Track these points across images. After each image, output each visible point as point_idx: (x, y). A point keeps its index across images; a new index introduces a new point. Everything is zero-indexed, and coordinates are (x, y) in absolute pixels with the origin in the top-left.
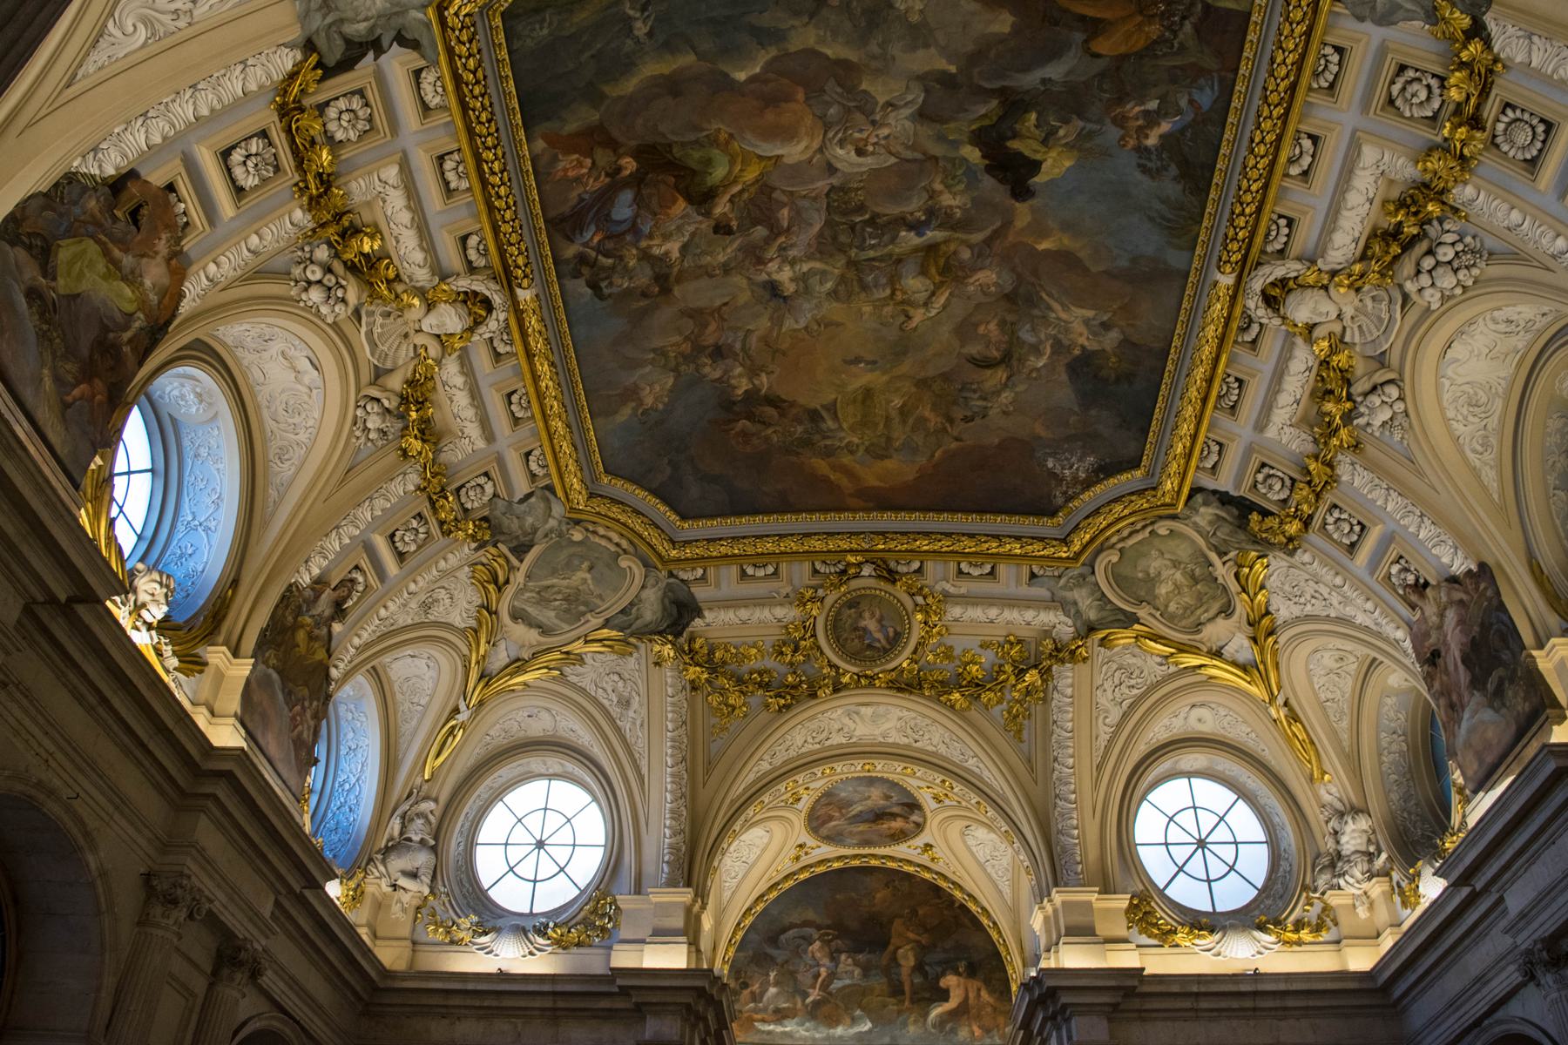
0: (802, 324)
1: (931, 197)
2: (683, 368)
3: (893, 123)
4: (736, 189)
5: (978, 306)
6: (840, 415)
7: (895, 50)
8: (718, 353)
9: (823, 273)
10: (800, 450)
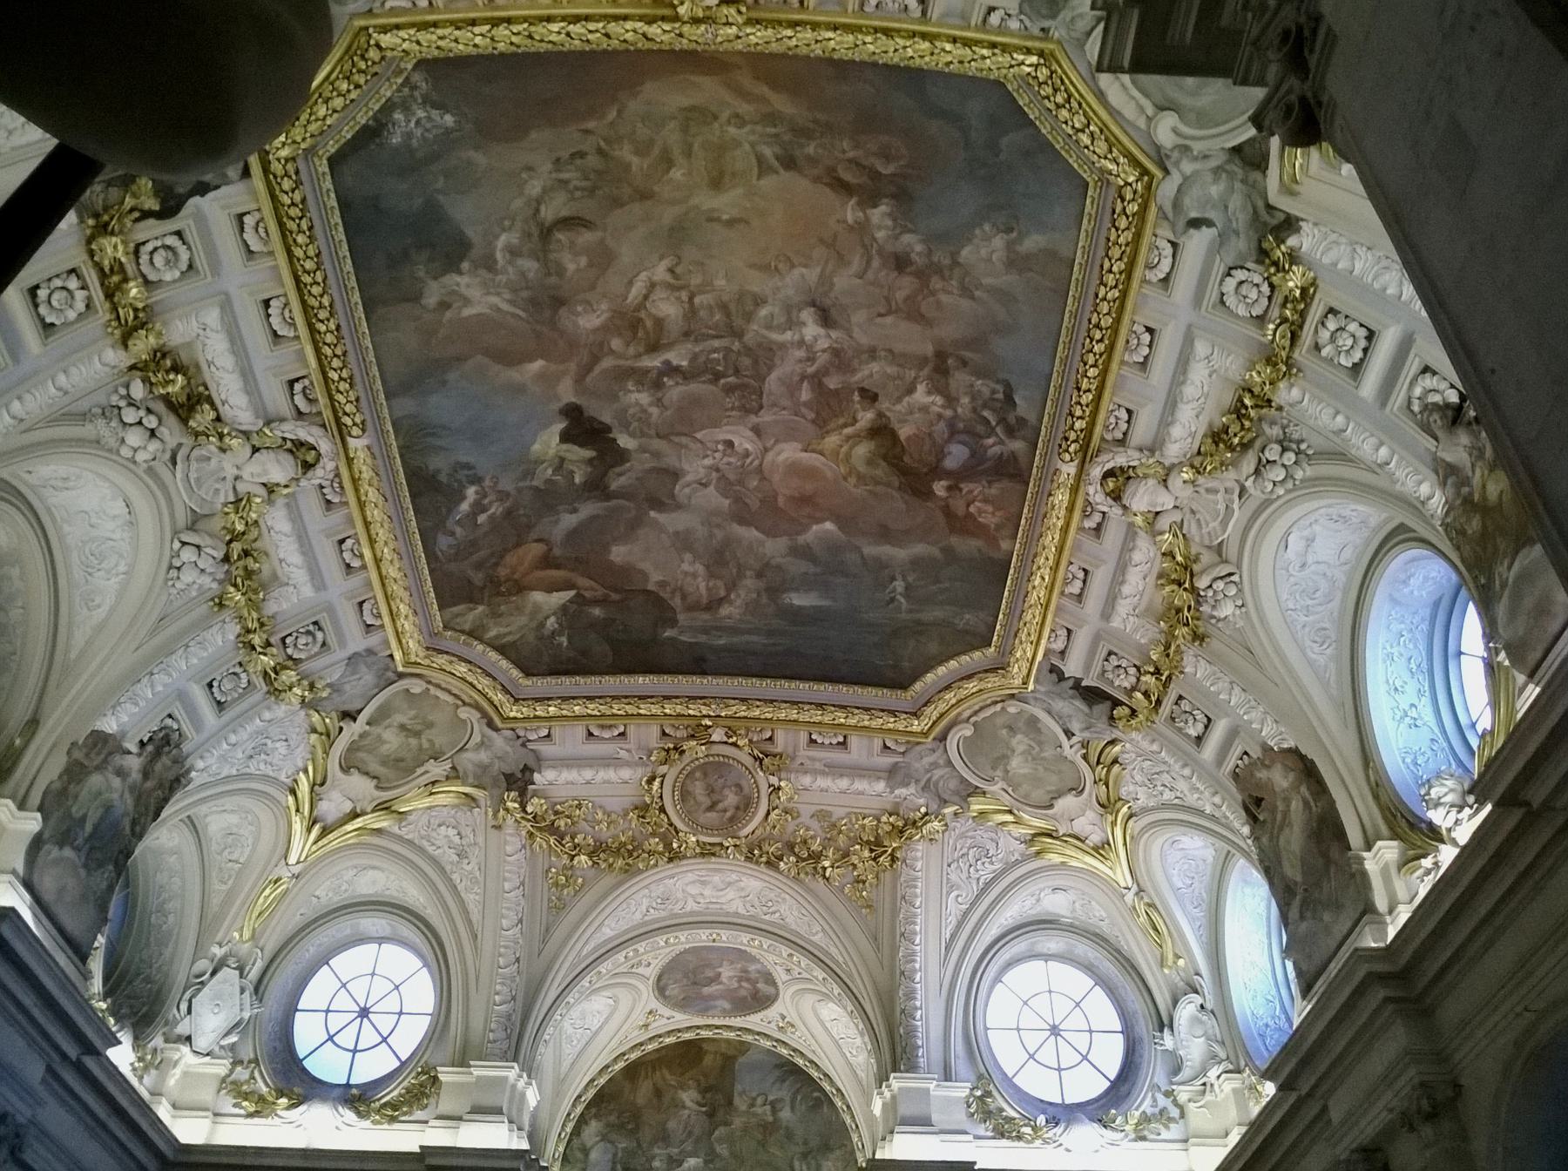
0: (797, 272)
1: (659, 400)
2: (947, 262)
3: (702, 470)
4: (848, 431)
5: (593, 287)
6: (754, 161)
7: (701, 532)
8: (900, 263)
9: (769, 327)
10: (811, 126)
